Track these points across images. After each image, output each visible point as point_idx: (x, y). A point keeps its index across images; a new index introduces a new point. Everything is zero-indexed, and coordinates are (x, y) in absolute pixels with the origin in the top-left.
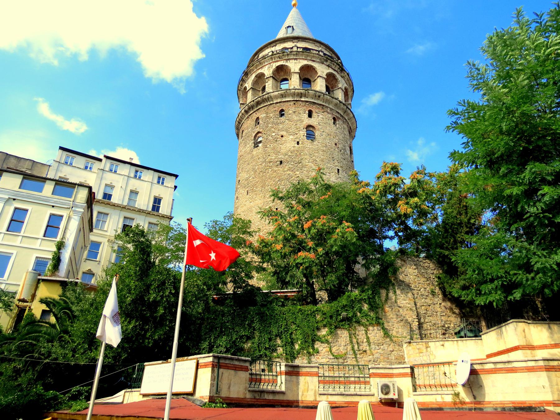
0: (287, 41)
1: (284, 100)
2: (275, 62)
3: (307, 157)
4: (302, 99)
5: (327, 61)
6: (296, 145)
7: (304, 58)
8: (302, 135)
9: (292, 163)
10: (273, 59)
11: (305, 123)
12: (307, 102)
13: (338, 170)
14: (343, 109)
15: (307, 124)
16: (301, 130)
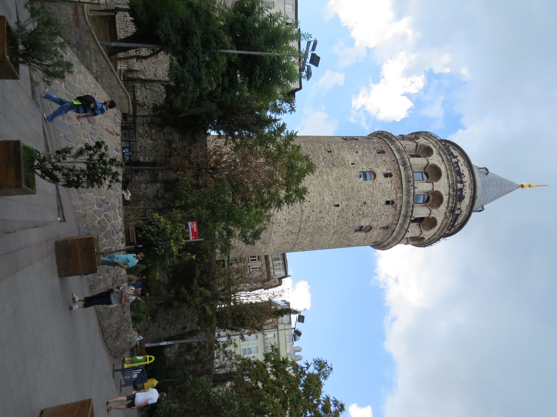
0: (463, 158)
1: (395, 153)
2: (434, 146)
3: (341, 173)
4: (400, 166)
5: (453, 191)
6: (350, 163)
7: (448, 167)
8: (363, 167)
9: (331, 159)
10: (437, 144)
11: (376, 169)
12: (400, 171)
13: (338, 206)
15: (375, 171)
16: (367, 167)
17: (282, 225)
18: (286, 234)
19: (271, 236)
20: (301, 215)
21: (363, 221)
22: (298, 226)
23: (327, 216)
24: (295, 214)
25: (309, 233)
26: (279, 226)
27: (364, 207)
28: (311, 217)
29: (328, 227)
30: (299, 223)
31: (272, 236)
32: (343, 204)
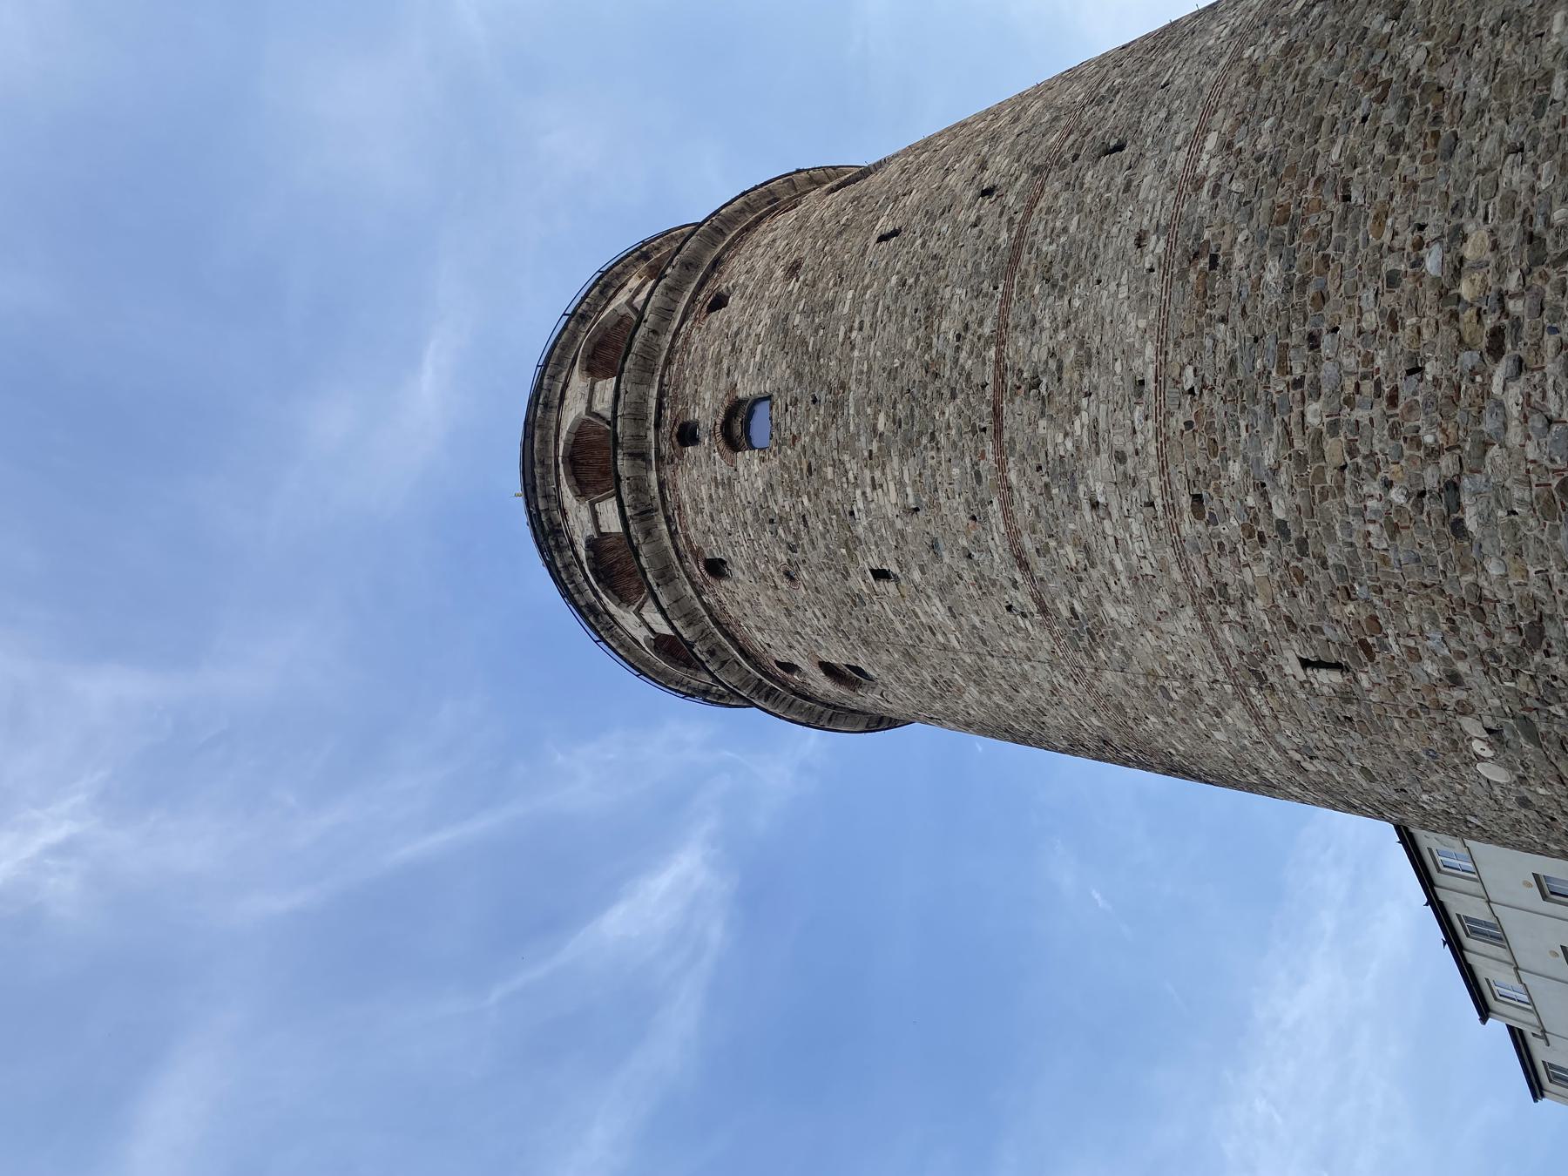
14: (648, 533)
17: (1103, 461)
18: (1066, 376)
19: (1161, 351)
20: (1018, 532)
21: (760, 483)
22: (1012, 449)
23: (899, 524)
24: (1053, 544)
25: (947, 393)
26: (1121, 457)
27: (785, 560)
28: (963, 516)
29: (875, 446)
30: (1013, 477)
31: (1150, 351)
32: (862, 583)
